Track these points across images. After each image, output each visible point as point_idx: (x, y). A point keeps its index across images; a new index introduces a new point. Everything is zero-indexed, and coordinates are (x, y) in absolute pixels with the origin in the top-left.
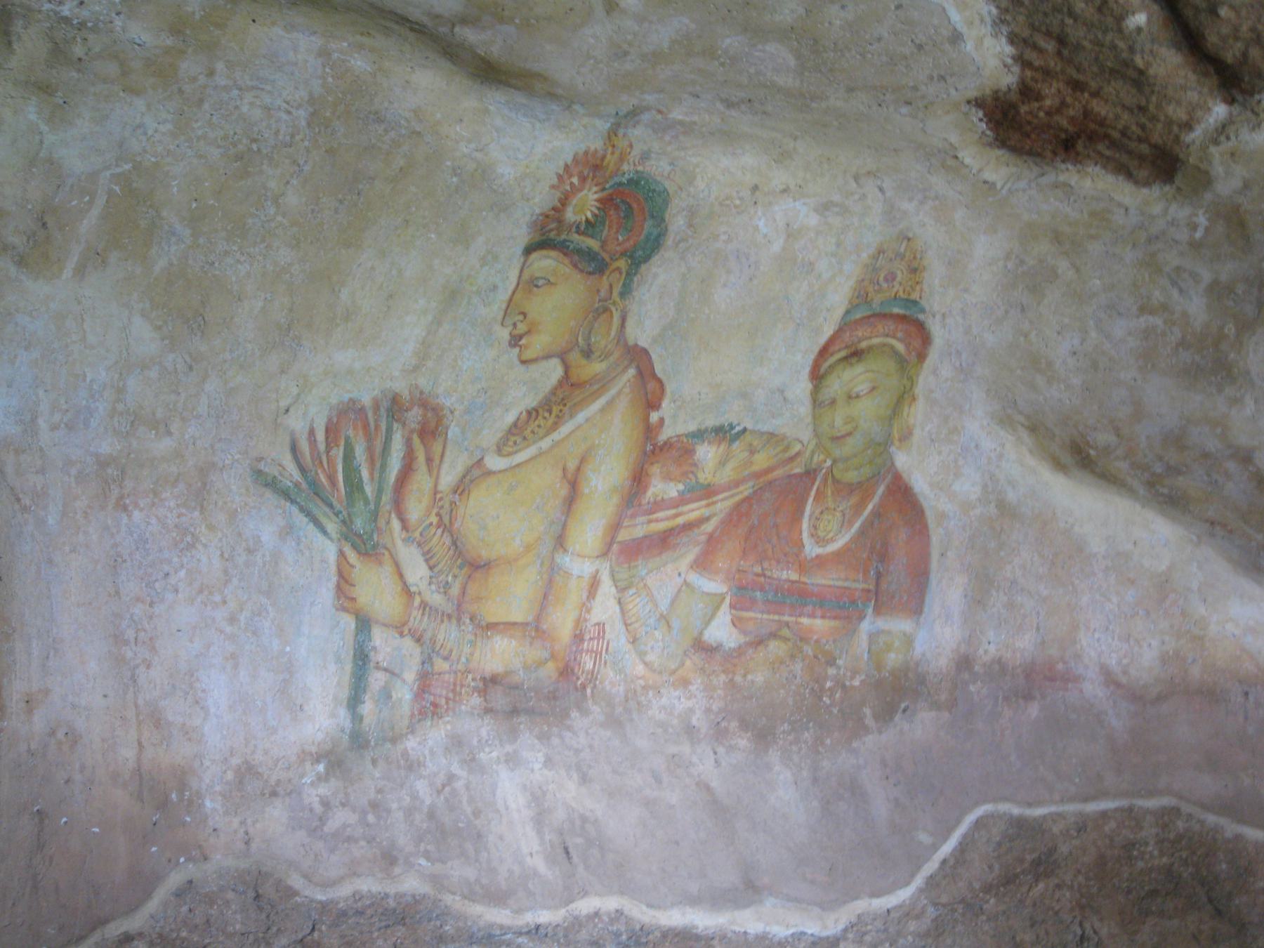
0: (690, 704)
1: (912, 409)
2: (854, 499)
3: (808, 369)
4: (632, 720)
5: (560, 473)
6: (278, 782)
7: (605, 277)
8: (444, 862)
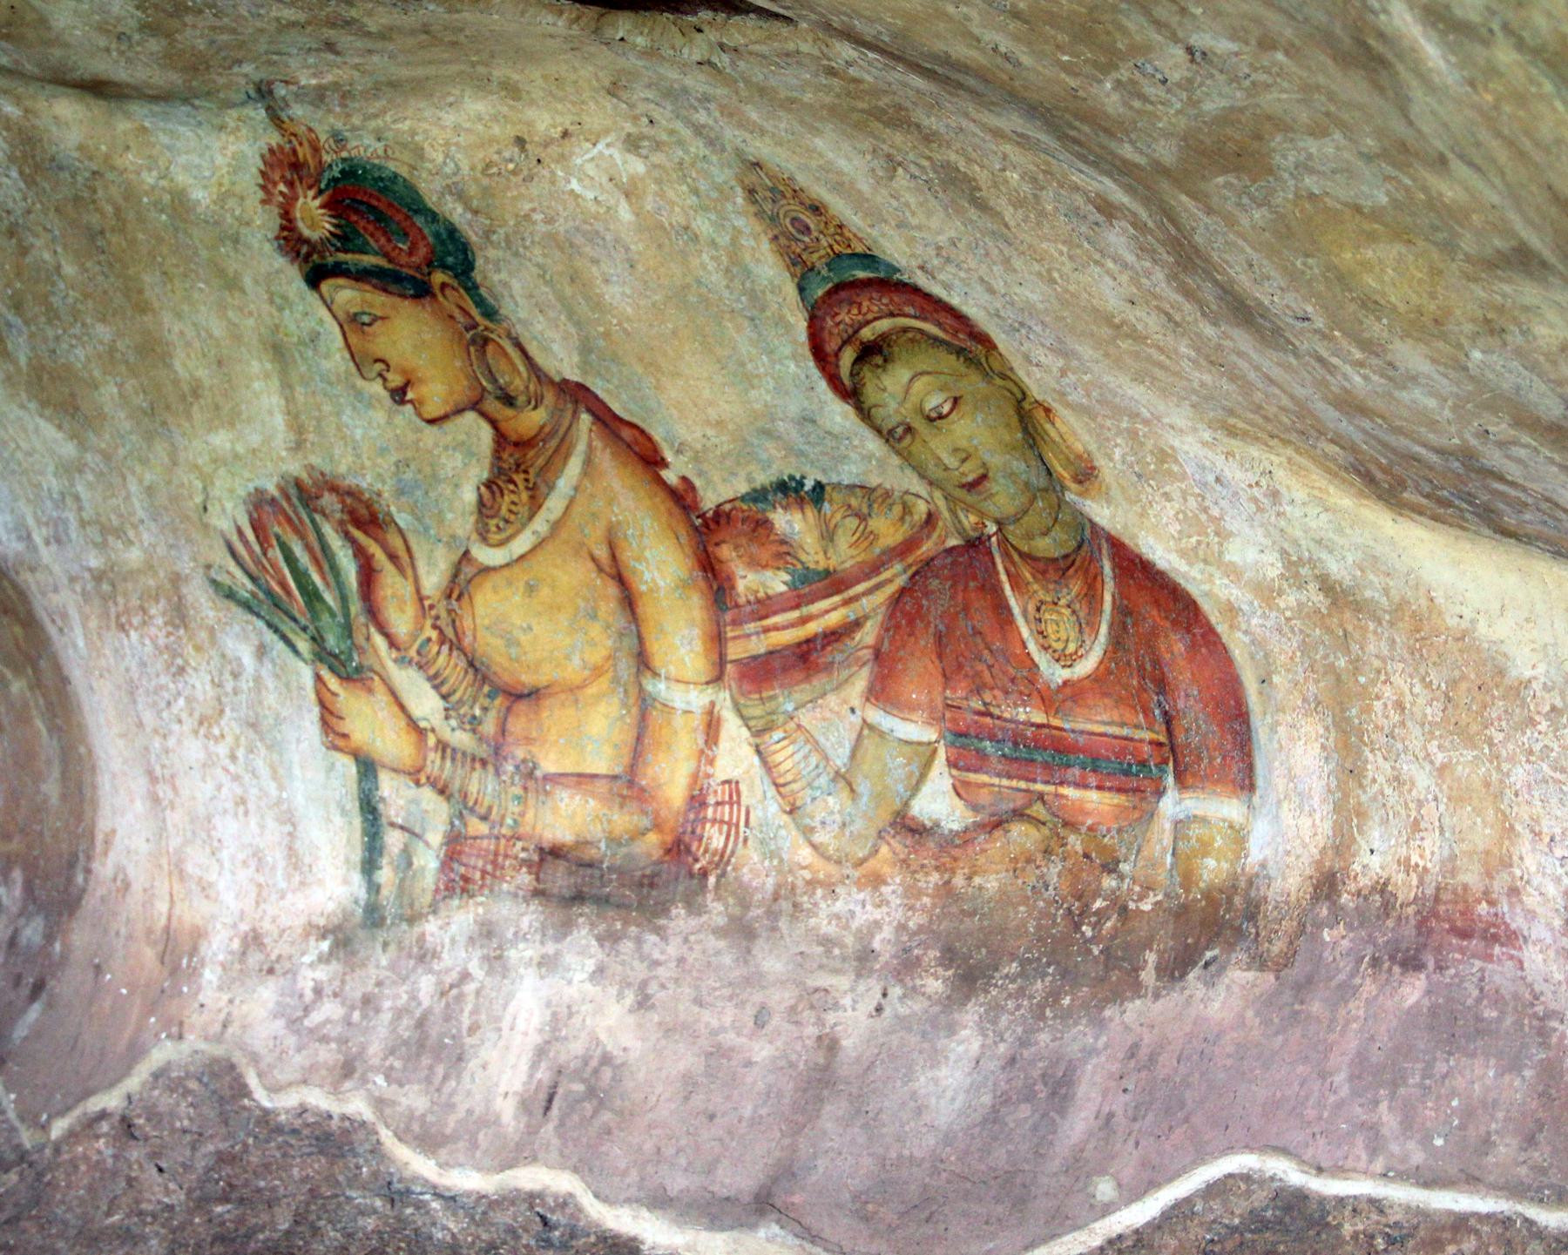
0: (878, 914)
1: (1058, 424)
2: (1076, 586)
3: (822, 385)
4: (774, 929)
5: (591, 565)
6: (279, 957)
8: (401, 1085)
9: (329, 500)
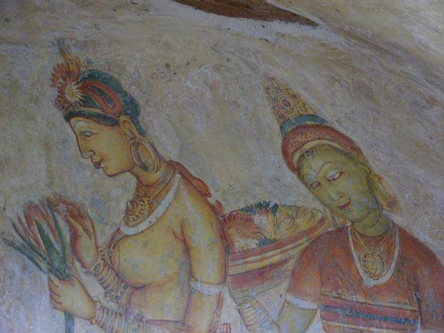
3: (285, 166)
5: (172, 235)
7: (122, 126)
9: (61, 207)
